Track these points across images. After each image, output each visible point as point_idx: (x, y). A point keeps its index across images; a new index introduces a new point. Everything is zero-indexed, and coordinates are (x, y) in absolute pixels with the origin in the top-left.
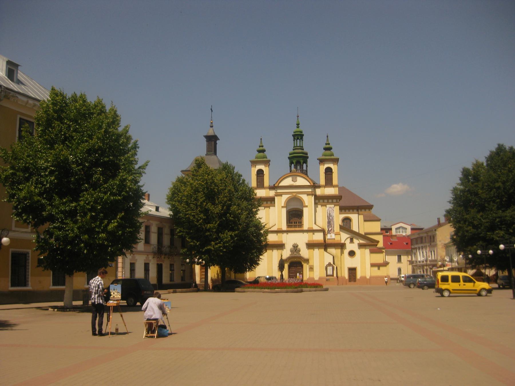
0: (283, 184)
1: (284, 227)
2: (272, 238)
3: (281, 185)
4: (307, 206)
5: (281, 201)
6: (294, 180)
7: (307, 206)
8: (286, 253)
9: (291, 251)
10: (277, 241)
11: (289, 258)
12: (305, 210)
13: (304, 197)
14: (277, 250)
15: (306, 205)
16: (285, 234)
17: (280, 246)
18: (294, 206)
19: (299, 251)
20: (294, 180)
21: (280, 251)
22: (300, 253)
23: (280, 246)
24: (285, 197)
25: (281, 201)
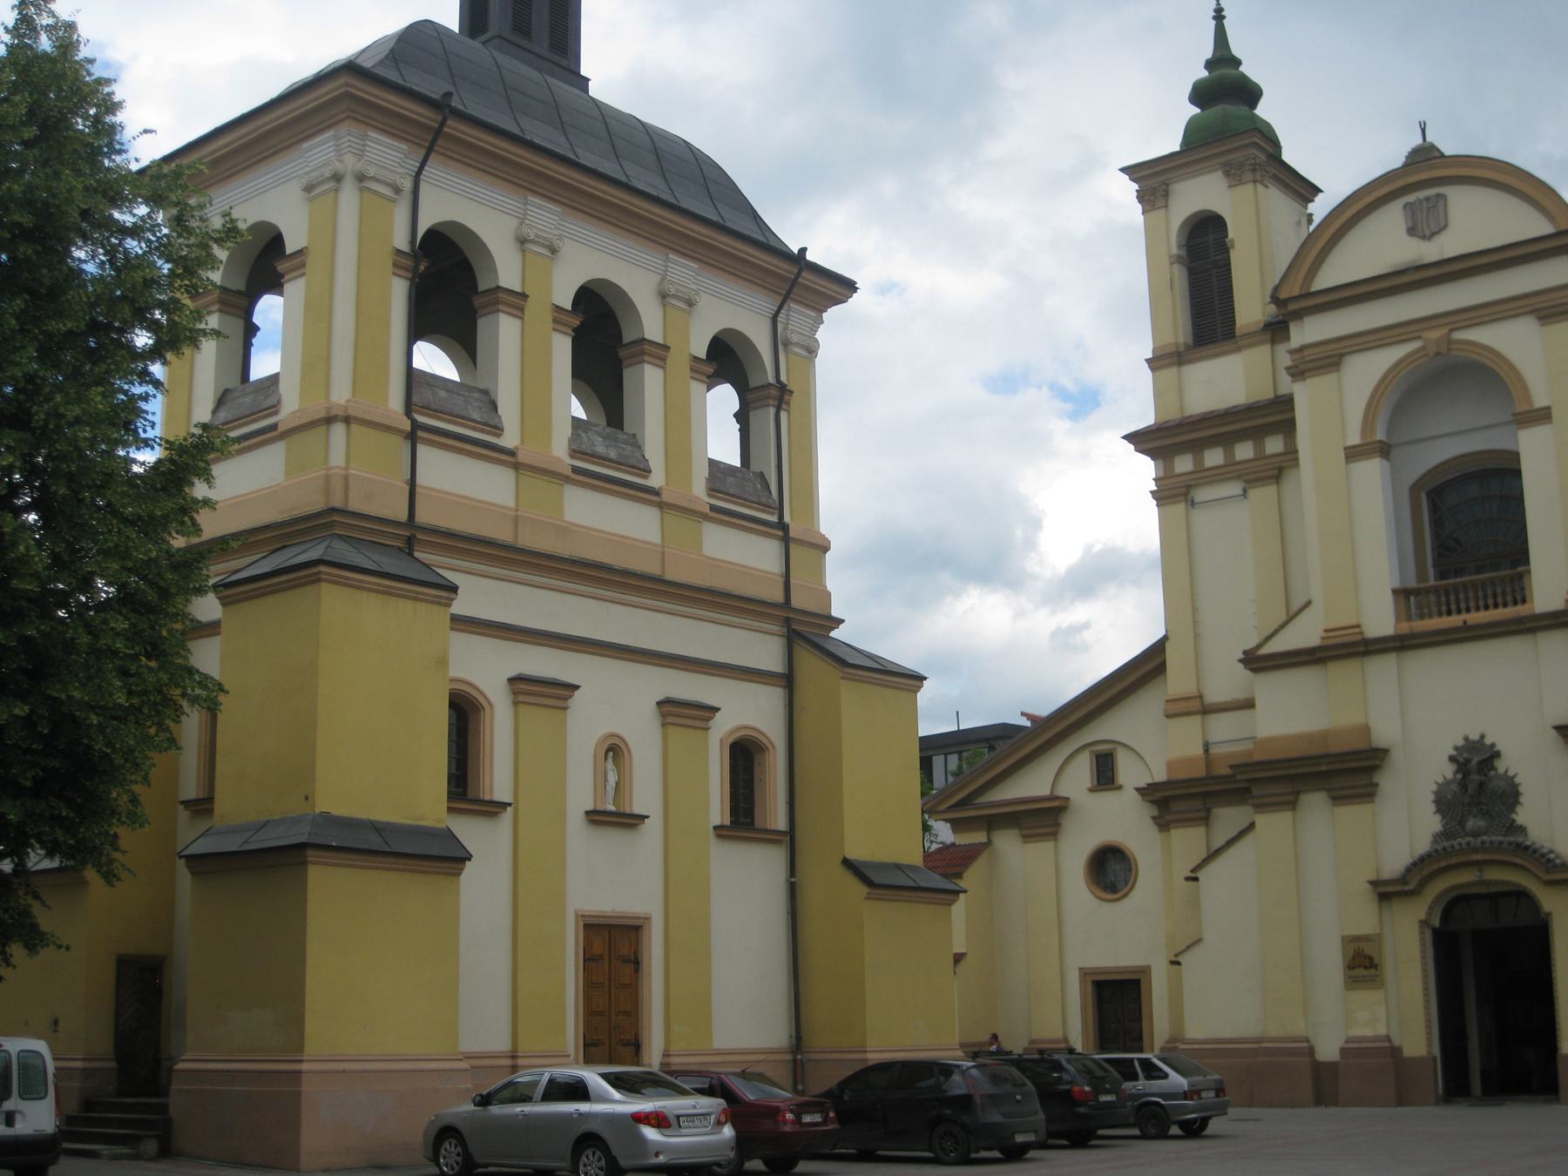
0: (1333, 274)
1: (1381, 620)
2: (1290, 712)
3: (1328, 278)
4: (1543, 416)
5: (1334, 409)
6: (1425, 224)
7: (1543, 416)
8: (1404, 822)
9: (1443, 803)
10: (1324, 735)
11: (1422, 870)
12: (1536, 453)
13: (1516, 342)
14: (1337, 799)
15: (1540, 401)
16: (1383, 668)
17: (1348, 770)
18: (1452, 437)
19: (1511, 795)
20: (1425, 224)
21: (1353, 813)
22: (1522, 816)
23: (1348, 770)
24: (1366, 372)
25: (1334, 409)
